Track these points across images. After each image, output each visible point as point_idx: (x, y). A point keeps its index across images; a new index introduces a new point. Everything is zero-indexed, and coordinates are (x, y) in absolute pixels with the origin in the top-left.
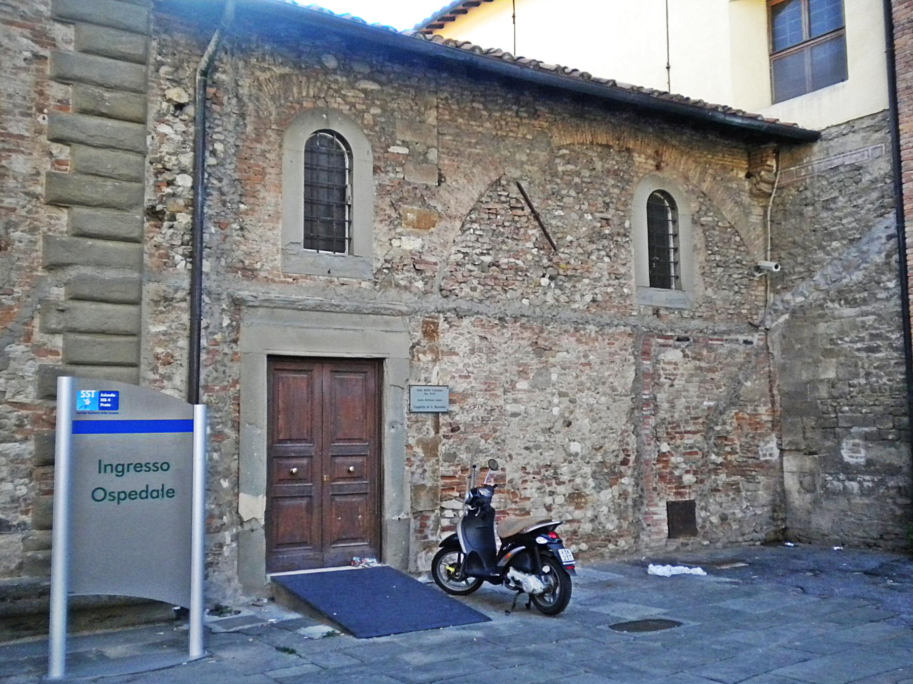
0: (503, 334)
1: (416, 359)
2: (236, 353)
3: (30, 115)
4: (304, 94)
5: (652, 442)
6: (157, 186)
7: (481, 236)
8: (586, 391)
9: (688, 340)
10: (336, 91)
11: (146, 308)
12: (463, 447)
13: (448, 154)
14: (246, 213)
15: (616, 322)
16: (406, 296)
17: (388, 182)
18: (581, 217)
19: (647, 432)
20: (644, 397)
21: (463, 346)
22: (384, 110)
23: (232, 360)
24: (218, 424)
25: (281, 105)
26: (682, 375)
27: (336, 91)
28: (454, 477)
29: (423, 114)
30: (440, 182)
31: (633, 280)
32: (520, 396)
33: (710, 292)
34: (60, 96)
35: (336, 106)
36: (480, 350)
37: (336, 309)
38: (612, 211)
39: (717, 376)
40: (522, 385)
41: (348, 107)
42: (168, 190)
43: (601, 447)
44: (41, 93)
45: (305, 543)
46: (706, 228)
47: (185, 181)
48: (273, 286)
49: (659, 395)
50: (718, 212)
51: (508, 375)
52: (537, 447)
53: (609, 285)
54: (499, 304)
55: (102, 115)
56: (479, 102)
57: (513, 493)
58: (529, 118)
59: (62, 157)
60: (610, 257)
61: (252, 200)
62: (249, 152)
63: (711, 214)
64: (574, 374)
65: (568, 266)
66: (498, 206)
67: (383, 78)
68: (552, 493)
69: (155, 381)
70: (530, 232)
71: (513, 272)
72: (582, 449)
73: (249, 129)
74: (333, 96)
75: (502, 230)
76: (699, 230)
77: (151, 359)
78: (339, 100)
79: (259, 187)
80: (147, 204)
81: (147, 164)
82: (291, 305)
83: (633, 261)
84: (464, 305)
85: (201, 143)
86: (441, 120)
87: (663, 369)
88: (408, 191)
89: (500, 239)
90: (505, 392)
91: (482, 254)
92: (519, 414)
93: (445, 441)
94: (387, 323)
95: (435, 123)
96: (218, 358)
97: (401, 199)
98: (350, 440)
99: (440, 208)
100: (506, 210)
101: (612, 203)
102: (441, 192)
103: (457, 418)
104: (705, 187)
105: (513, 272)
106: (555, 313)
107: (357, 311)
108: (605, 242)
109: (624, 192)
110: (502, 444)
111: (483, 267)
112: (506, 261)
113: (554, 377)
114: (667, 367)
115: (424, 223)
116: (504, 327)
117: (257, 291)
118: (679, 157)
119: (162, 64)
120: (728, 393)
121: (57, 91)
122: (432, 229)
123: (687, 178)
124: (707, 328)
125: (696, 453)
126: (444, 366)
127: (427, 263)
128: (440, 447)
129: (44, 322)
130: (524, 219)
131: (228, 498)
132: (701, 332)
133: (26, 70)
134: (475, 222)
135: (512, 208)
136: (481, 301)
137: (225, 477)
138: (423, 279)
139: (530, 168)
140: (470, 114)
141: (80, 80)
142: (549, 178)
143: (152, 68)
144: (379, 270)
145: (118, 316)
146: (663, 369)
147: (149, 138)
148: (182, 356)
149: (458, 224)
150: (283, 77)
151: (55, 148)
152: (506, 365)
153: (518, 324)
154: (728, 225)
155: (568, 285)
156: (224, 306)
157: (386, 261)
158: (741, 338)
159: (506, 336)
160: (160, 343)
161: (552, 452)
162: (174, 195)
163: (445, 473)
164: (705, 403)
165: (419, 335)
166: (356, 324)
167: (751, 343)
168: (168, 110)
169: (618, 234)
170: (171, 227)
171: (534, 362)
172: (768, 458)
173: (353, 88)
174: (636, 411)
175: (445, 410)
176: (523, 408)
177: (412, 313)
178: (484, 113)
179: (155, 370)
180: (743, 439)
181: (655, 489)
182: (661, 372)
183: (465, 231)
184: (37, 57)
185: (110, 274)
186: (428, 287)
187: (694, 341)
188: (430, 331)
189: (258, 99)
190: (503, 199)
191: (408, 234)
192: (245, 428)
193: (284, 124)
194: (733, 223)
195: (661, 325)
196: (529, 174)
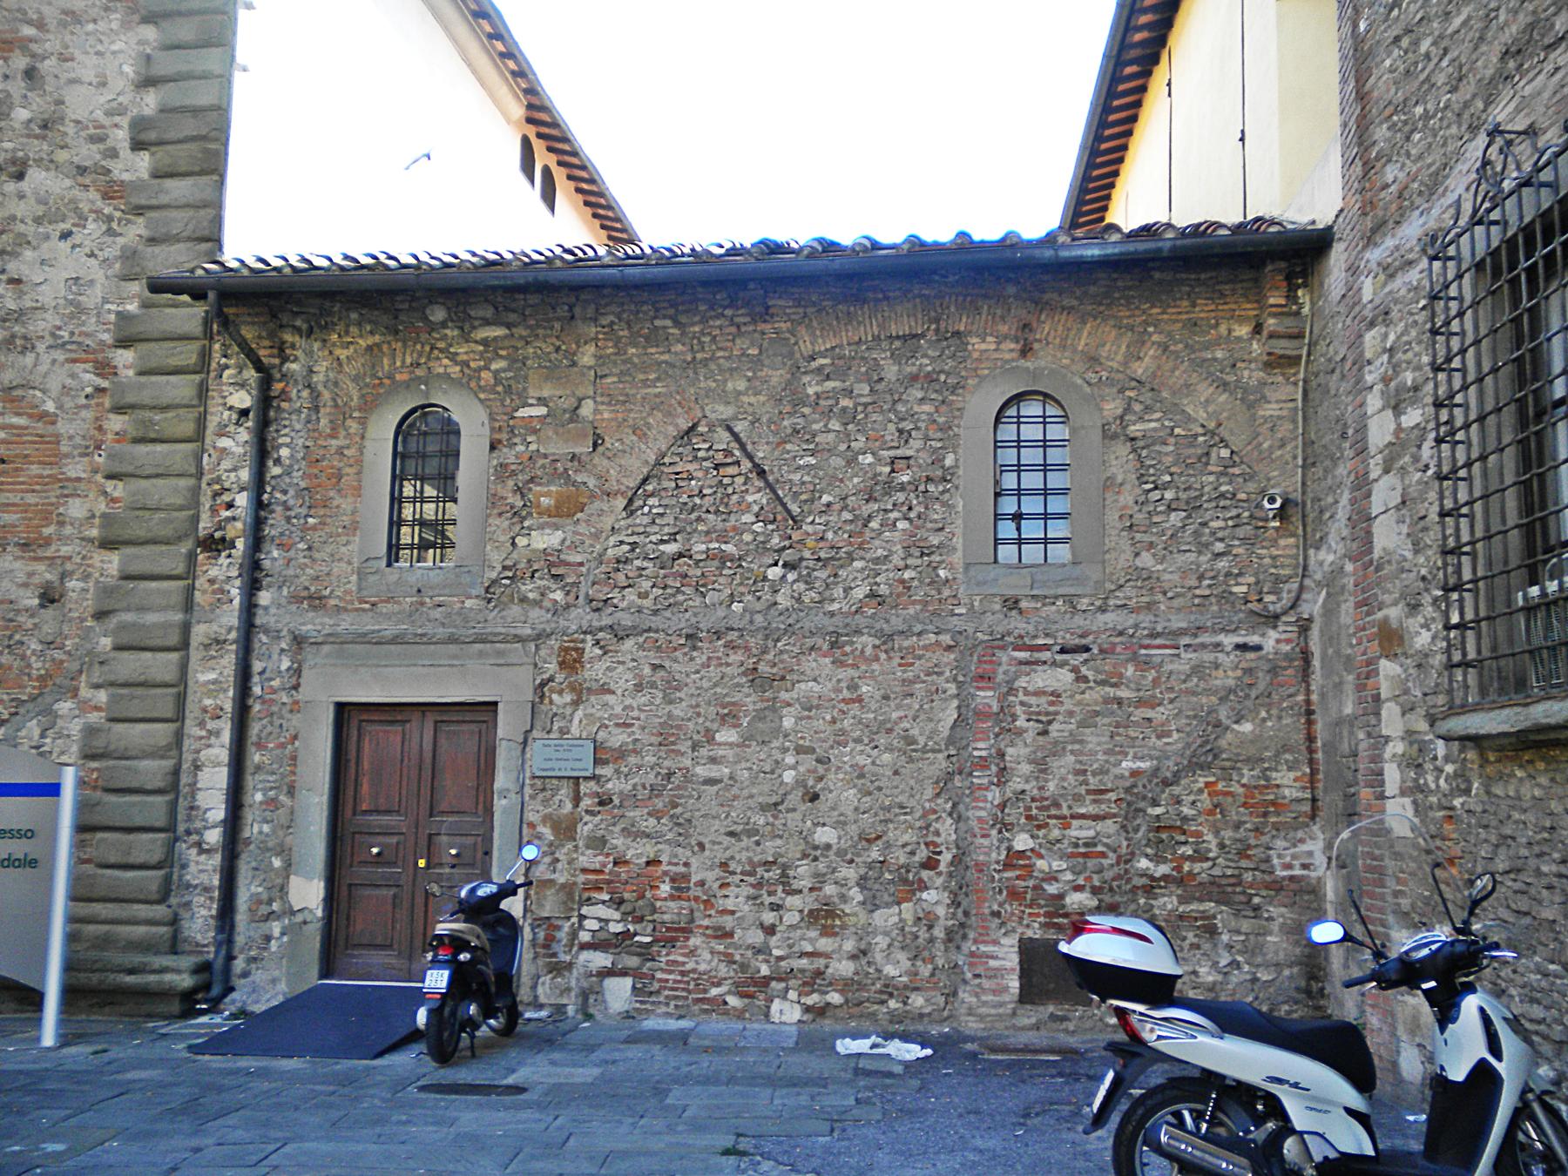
1: (547, 701)
2: (296, 702)
4: (398, 364)
5: (994, 832)
6: (214, 511)
8: (851, 745)
9: (1087, 649)
10: (441, 351)
11: (195, 655)
12: (617, 829)
13: (609, 404)
14: (314, 528)
15: (918, 628)
16: (535, 613)
17: (513, 460)
18: (851, 461)
19: (983, 814)
20: (976, 753)
21: (623, 680)
22: (512, 360)
24: (271, 789)
26: (1071, 714)
27: (441, 351)
28: (601, 872)
29: (574, 354)
30: (595, 445)
31: (959, 554)
32: (721, 753)
33: (1146, 559)
34: (117, 427)
35: (441, 370)
36: (653, 685)
37: (424, 640)
38: (916, 444)
39: (1158, 714)
40: (726, 735)
41: (458, 368)
42: (228, 513)
43: (879, 837)
44: (100, 428)
45: (390, 947)
46: (1141, 443)
47: (242, 500)
48: (344, 616)
49: (1010, 751)
50: (1173, 409)
51: (701, 720)
52: (751, 833)
53: (907, 567)
54: (687, 615)
55: (153, 441)
56: (665, 317)
57: (706, 902)
58: (754, 321)
59: (116, 494)
62: (322, 452)
63: (1158, 415)
64: (828, 717)
65: (821, 544)
66: (691, 467)
67: (513, 317)
68: (776, 907)
69: (201, 738)
70: (750, 498)
71: (716, 563)
72: (840, 838)
73: (323, 422)
74: (438, 358)
75: (697, 501)
76: (1123, 449)
77: (197, 713)
78: (446, 361)
80: (202, 533)
81: (204, 485)
82: (362, 638)
83: (959, 522)
84: (627, 620)
85: (262, 452)
87: (1022, 704)
88: (543, 467)
91: (662, 542)
92: (721, 781)
93: (587, 818)
94: (500, 653)
95: (592, 362)
96: (275, 709)
97: (532, 480)
99: (592, 483)
100: (707, 472)
101: (917, 428)
102: (596, 460)
103: (610, 785)
104: (1139, 369)
105: (716, 563)
106: (791, 621)
107: (452, 640)
108: (901, 497)
109: (944, 408)
111: (663, 562)
112: (703, 547)
113: (788, 723)
114: (1033, 700)
115: (567, 509)
116: (694, 648)
117: (323, 624)
119: (227, 367)
120: (1188, 745)
121: (116, 423)
122: (579, 515)
123: (1093, 360)
124: (1136, 626)
125: (1103, 855)
126: (590, 711)
127: (568, 564)
128: (579, 826)
130: (739, 480)
131: (279, 881)
132: (1121, 634)
133: (86, 407)
134: (652, 495)
135: (717, 467)
136: (656, 612)
137: (277, 855)
139: (752, 399)
140: (647, 339)
141: (133, 407)
142: (788, 409)
144: (494, 582)
145: (162, 665)
146: (1022, 704)
149: (621, 502)
150: (369, 348)
151: (109, 485)
152: (698, 706)
154: (1200, 430)
155: (822, 574)
156: (284, 645)
158: (1229, 640)
159: (698, 661)
160: (209, 694)
161: (779, 842)
162: (234, 519)
163: (587, 866)
164: (1124, 764)
165: (552, 667)
166: (455, 657)
167: (1258, 648)
169: (929, 479)
170: (229, 556)
171: (750, 701)
172: (1297, 872)
173: (467, 341)
174: (957, 777)
175: (587, 774)
176: (727, 771)
177: (540, 637)
178: (676, 331)
179: (202, 724)
180: (1228, 834)
181: (997, 914)
182: (1019, 710)
183: (632, 513)
184: (100, 390)
185: (151, 618)
187: (1102, 651)
188: (571, 661)
189: (336, 384)
190: (701, 454)
191: (541, 527)
192: (302, 795)
193: (369, 405)
195: (1017, 624)
196: (750, 410)
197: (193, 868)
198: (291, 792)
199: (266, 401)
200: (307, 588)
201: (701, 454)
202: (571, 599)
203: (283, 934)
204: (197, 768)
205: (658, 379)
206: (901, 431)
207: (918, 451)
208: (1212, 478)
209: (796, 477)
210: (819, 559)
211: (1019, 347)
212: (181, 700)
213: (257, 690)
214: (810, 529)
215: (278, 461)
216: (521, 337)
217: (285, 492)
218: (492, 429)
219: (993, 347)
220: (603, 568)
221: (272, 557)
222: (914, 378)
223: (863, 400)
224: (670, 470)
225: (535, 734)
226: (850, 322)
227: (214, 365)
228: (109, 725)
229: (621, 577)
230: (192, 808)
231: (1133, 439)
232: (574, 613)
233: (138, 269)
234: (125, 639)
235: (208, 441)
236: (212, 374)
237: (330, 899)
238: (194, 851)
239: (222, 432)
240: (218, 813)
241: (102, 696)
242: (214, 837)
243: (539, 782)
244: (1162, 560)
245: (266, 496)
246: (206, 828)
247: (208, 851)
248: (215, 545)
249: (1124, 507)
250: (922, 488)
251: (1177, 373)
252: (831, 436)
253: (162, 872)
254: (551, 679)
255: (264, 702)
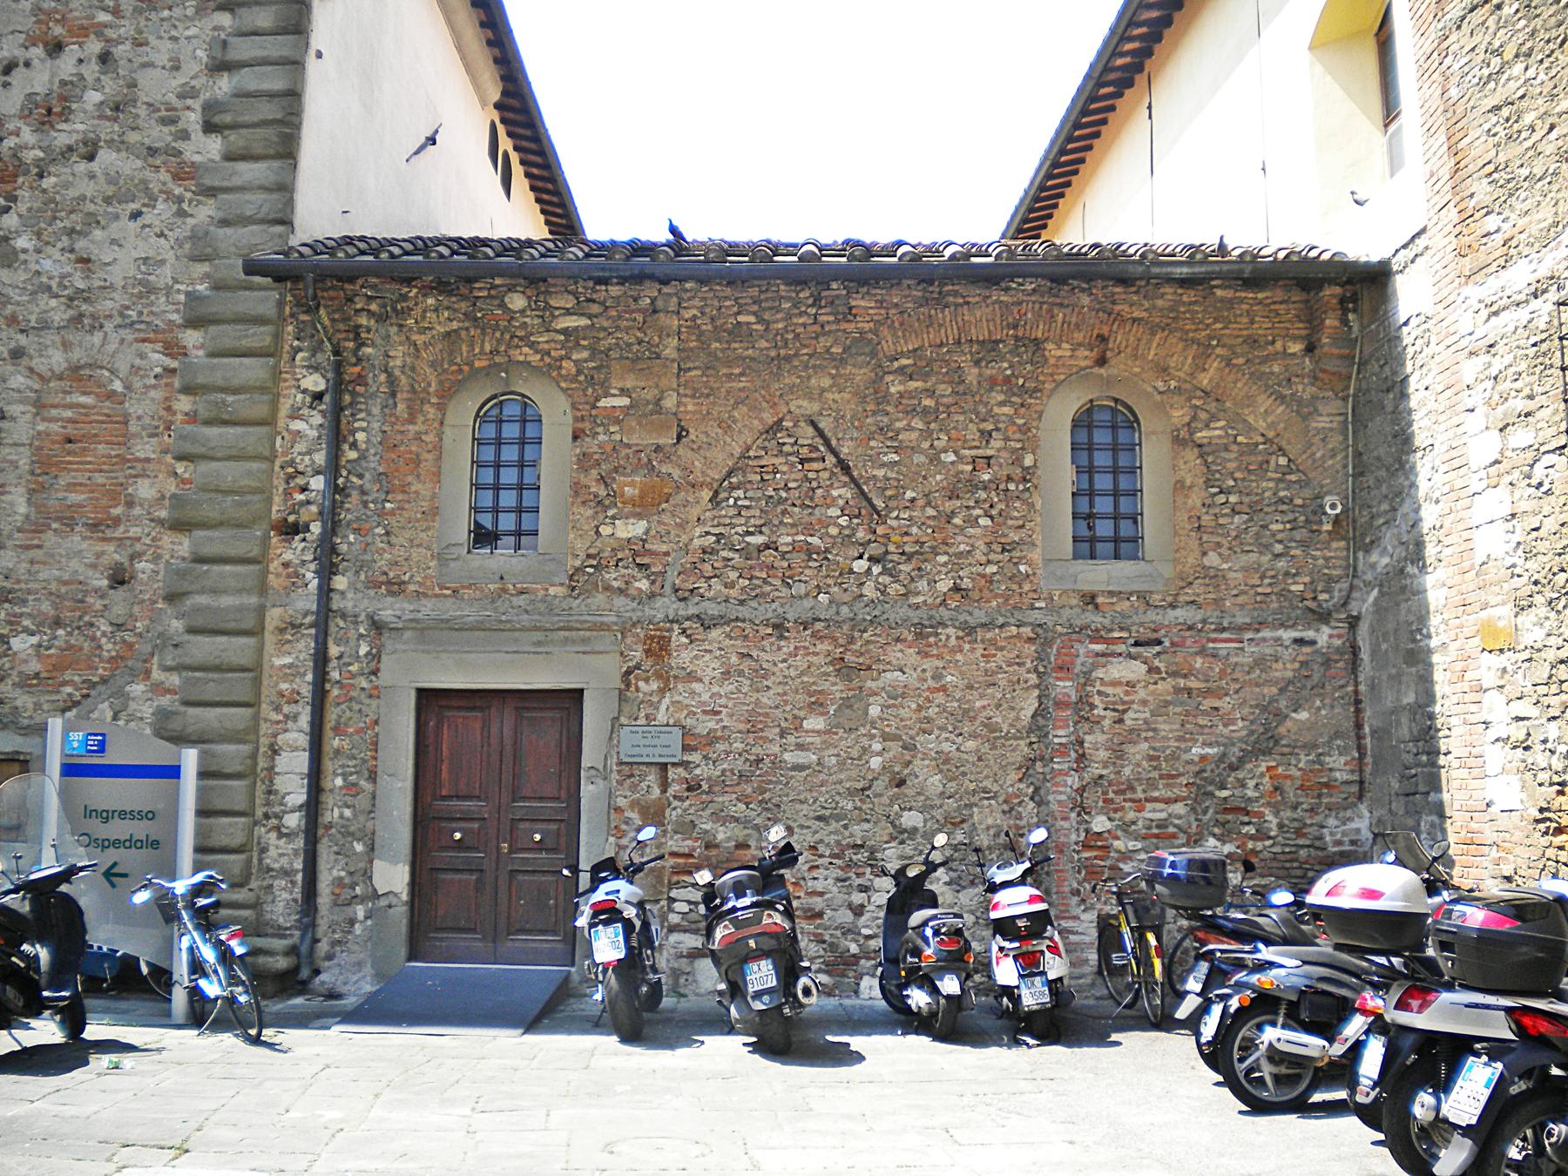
0: (779, 649)
1: (633, 688)
2: (376, 688)
3: (156, 435)
5: (1073, 815)
6: (288, 494)
7: (747, 507)
8: (936, 732)
9: (1160, 643)
10: (521, 339)
11: (270, 638)
13: (693, 396)
14: (392, 513)
15: (1001, 620)
16: (620, 602)
17: (596, 449)
18: (935, 459)
19: (1063, 797)
20: (1056, 740)
21: (709, 667)
23: (371, 696)
25: (445, 371)
26: (1144, 703)
27: (521, 339)
28: (690, 856)
30: (679, 437)
32: (809, 740)
33: (1212, 559)
35: (521, 358)
36: (741, 673)
38: (996, 443)
39: (1225, 704)
40: (814, 723)
41: (538, 357)
42: (302, 497)
43: (963, 821)
44: (169, 409)
45: (474, 931)
47: (318, 483)
48: (424, 601)
49: (1087, 738)
50: (1236, 420)
51: (788, 708)
52: (838, 818)
53: (989, 562)
54: (774, 606)
55: (225, 423)
58: (837, 321)
60: (991, 517)
61: (400, 497)
62: (399, 437)
63: (1222, 423)
64: (914, 706)
65: (906, 539)
66: (777, 461)
68: (864, 889)
69: (278, 722)
70: (835, 493)
72: (925, 821)
73: (401, 407)
74: (517, 347)
75: (784, 495)
76: (1191, 455)
78: (526, 350)
79: (410, 479)
80: (274, 516)
81: (277, 468)
84: (713, 610)
85: (337, 436)
86: (684, 350)
87: (1099, 693)
89: (779, 509)
90: (782, 734)
92: (809, 767)
93: (676, 803)
94: (584, 641)
95: (674, 355)
96: (353, 694)
97: (616, 470)
98: (541, 799)
99: (676, 473)
100: (792, 465)
101: (997, 429)
103: (698, 771)
104: (1205, 380)
106: (876, 613)
108: (982, 495)
110: (776, 810)
111: (745, 551)
112: (789, 539)
113: (874, 711)
114: (1109, 690)
116: (781, 637)
117: (403, 610)
118: (1146, 337)
119: (300, 350)
120: (1252, 732)
121: (184, 404)
122: (664, 505)
123: (1163, 370)
124: (1204, 621)
125: (1174, 836)
126: (677, 698)
127: (652, 553)
128: (668, 812)
129: (161, 660)
130: (825, 475)
131: (362, 865)
132: (1190, 628)
136: (742, 603)
137: (359, 840)
138: (648, 577)
139: (837, 396)
143: (286, 357)
145: (236, 649)
146: (1099, 693)
147: (279, 439)
148: (306, 691)
149: (706, 494)
152: (785, 694)
153: (808, 632)
154: (1261, 439)
156: (362, 631)
157: (589, 556)
158: (1288, 635)
160: (285, 678)
161: (866, 826)
162: (309, 502)
163: (675, 849)
164: (1194, 750)
165: (637, 655)
166: (539, 643)
167: (1313, 643)
168: (303, 403)
169: (1009, 478)
171: (837, 689)
174: (1038, 764)
175: (675, 760)
176: (814, 757)
179: (278, 709)
180: (1287, 814)
181: (1077, 892)
182: (1097, 700)
183: (718, 504)
185: (226, 601)
186: (656, 588)
187: (1173, 644)
188: (658, 648)
189: (413, 369)
190: (787, 449)
192: (383, 779)
193: (447, 394)
194: (1271, 434)
195: (1096, 619)
196: (834, 406)
197: (273, 852)
198: (373, 777)
199: (339, 384)
200: (385, 573)
201: (787, 449)
202: (656, 588)
203: (366, 918)
204: (276, 752)
205: (742, 374)
206: (982, 432)
207: (999, 450)
208: (1271, 484)
209: (880, 473)
210: (903, 553)
211: (1094, 354)
212: (257, 682)
213: (335, 675)
214: (894, 523)
215: (354, 445)
216: (605, 329)
217: (361, 476)
218: (576, 419)
219: (1068, 353)
220: (690, 558)
221: (347, 542)
222: (993, 382)
223: (945, 400)
224: (755, 463)
225: (623, 720)
226: (931, 324)
227: (287, 348)
228: (183, 709)
229: (707, 568)
230: (270, 792)
231: (1200, 446)
232: (659, 602)
233: (209, 250)
234: (199, 622)
235: (281, 423)
236: (286, 357)
237: (414, 884)
238: (273, 835)
239: (295, 415)
240: (299, 797)
241: (175, 680)
242: (293, 821)
243: (626, 769)
244: (1225, 559)
245: (340, 481)
246: (285, 812)
247: (286, 835)
248: (291, 530)
249: (1193, 508)
250: (1002, 486)
251: (1239, 385)
252: (914, 435)
253: (242, 857)
254: (638, 667)
255: (342, 687)
